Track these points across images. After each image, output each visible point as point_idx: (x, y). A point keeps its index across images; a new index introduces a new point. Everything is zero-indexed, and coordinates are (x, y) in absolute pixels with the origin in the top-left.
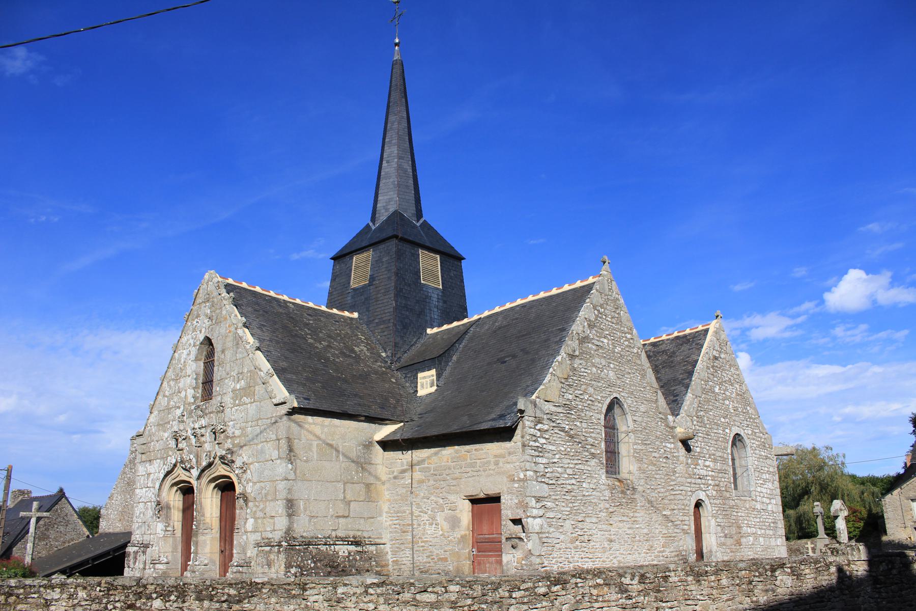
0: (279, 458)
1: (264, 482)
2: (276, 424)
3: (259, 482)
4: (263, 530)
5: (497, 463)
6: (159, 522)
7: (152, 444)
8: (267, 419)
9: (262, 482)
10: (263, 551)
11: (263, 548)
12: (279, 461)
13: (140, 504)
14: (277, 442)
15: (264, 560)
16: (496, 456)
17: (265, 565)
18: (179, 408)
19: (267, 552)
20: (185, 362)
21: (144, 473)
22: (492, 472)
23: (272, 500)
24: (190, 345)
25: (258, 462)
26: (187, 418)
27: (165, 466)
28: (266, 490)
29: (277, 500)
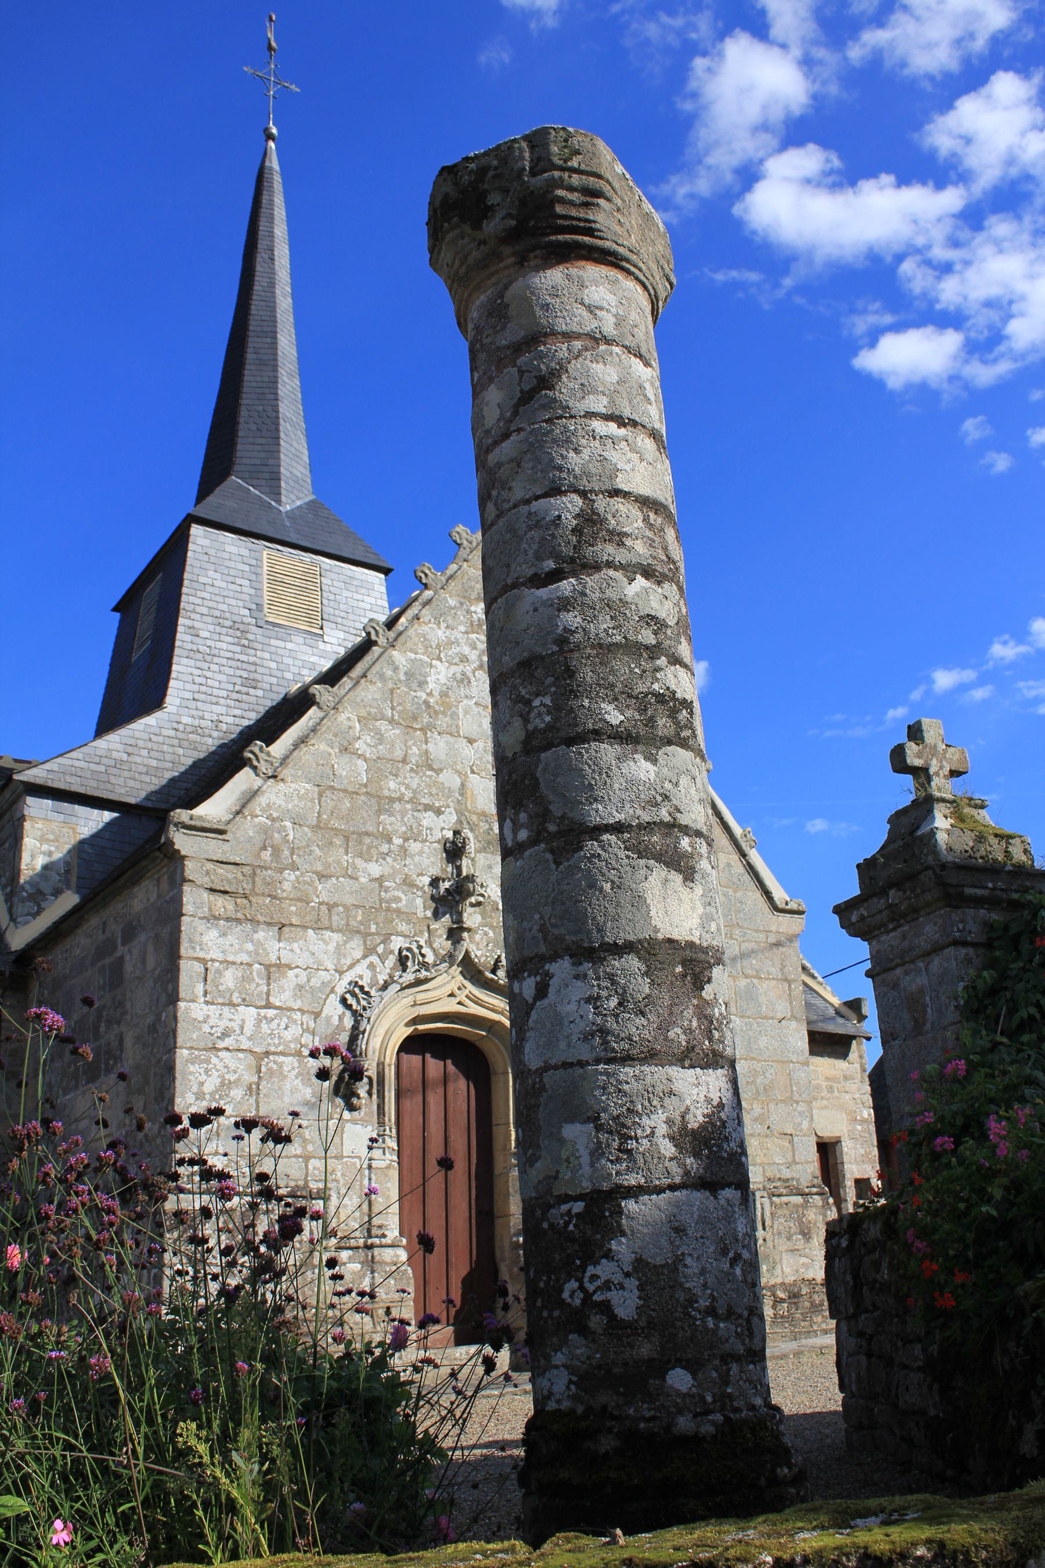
0: (794, 1017)
1: (759, 1061)
2: (781, 949)
3: (745, 1059)
4: (765, 1161)
5: (830, 1089)
6: (354, 1122)
7: (290, 876)
8: (757, 931)
9: (753, 1059)
10: (786, 1204)
11: (784, 1199)
12: (794, 1024)
13: (222, 1054)
14: (786, 985)
15: (792, 1225)
16: (827, 1079)
17: (796, 1233)
18: (438, 812)
19: (796, 1206)
20: (444, 695)
21: (244, 958)
22: (825, 1102)
23: (783, 1101)
24: (464, 659)
25: (742, 1017)
26: (478, 851)
27: (374, 959)
28: (765, 1077)
29: (797, 1102)
